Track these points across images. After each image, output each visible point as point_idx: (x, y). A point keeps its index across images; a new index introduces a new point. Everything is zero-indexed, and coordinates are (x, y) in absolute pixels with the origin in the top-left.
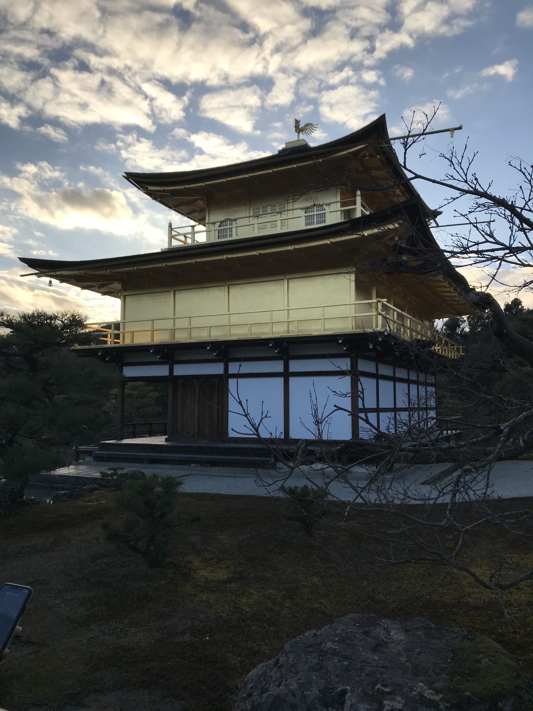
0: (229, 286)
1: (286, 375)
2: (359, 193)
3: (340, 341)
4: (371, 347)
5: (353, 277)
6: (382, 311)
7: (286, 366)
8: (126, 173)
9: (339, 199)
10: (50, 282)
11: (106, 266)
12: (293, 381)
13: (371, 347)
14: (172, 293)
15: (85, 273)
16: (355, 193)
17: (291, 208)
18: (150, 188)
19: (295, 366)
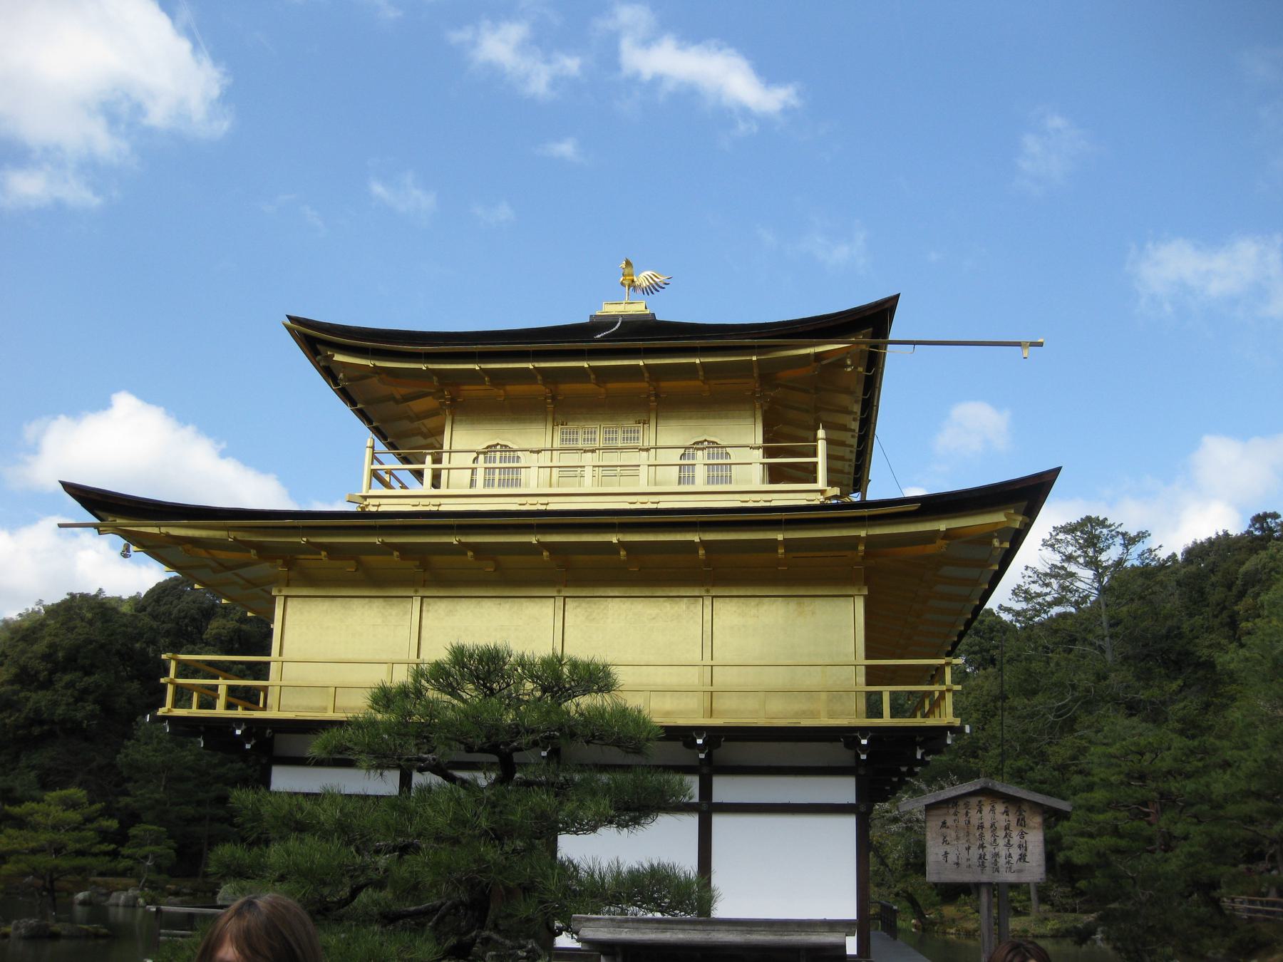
0: (565, 597)
1: (706, 810)
2: (821, 433)
3: (864, 742)
4: (919, 756)
5: (860, 605)
6: (954, 682)
7: (706, 790)
8: (289, 317)
9: (760, 441)
10: (127, 549)
11: (304, 527)
12: (718, 821)
13: (919, 756)
14: (417, 603)
15: (235, 539)
16: (816, 435)
17: (653, 444)
18: (339, 358)
19: (724, 789)
